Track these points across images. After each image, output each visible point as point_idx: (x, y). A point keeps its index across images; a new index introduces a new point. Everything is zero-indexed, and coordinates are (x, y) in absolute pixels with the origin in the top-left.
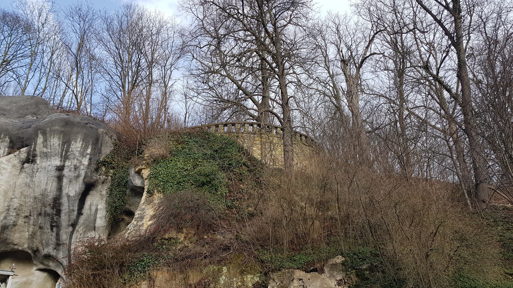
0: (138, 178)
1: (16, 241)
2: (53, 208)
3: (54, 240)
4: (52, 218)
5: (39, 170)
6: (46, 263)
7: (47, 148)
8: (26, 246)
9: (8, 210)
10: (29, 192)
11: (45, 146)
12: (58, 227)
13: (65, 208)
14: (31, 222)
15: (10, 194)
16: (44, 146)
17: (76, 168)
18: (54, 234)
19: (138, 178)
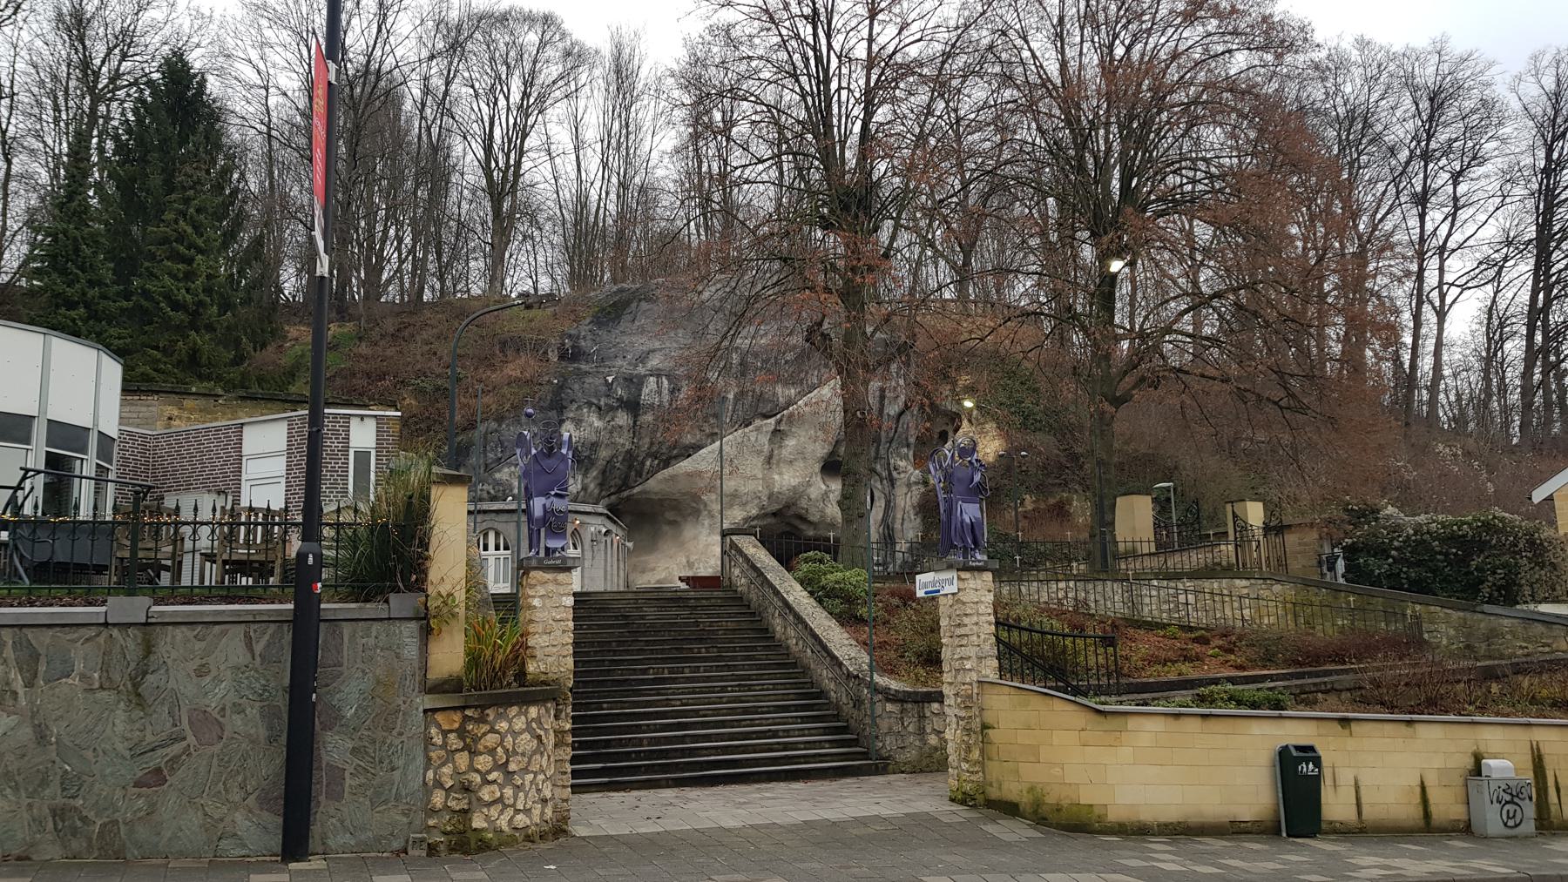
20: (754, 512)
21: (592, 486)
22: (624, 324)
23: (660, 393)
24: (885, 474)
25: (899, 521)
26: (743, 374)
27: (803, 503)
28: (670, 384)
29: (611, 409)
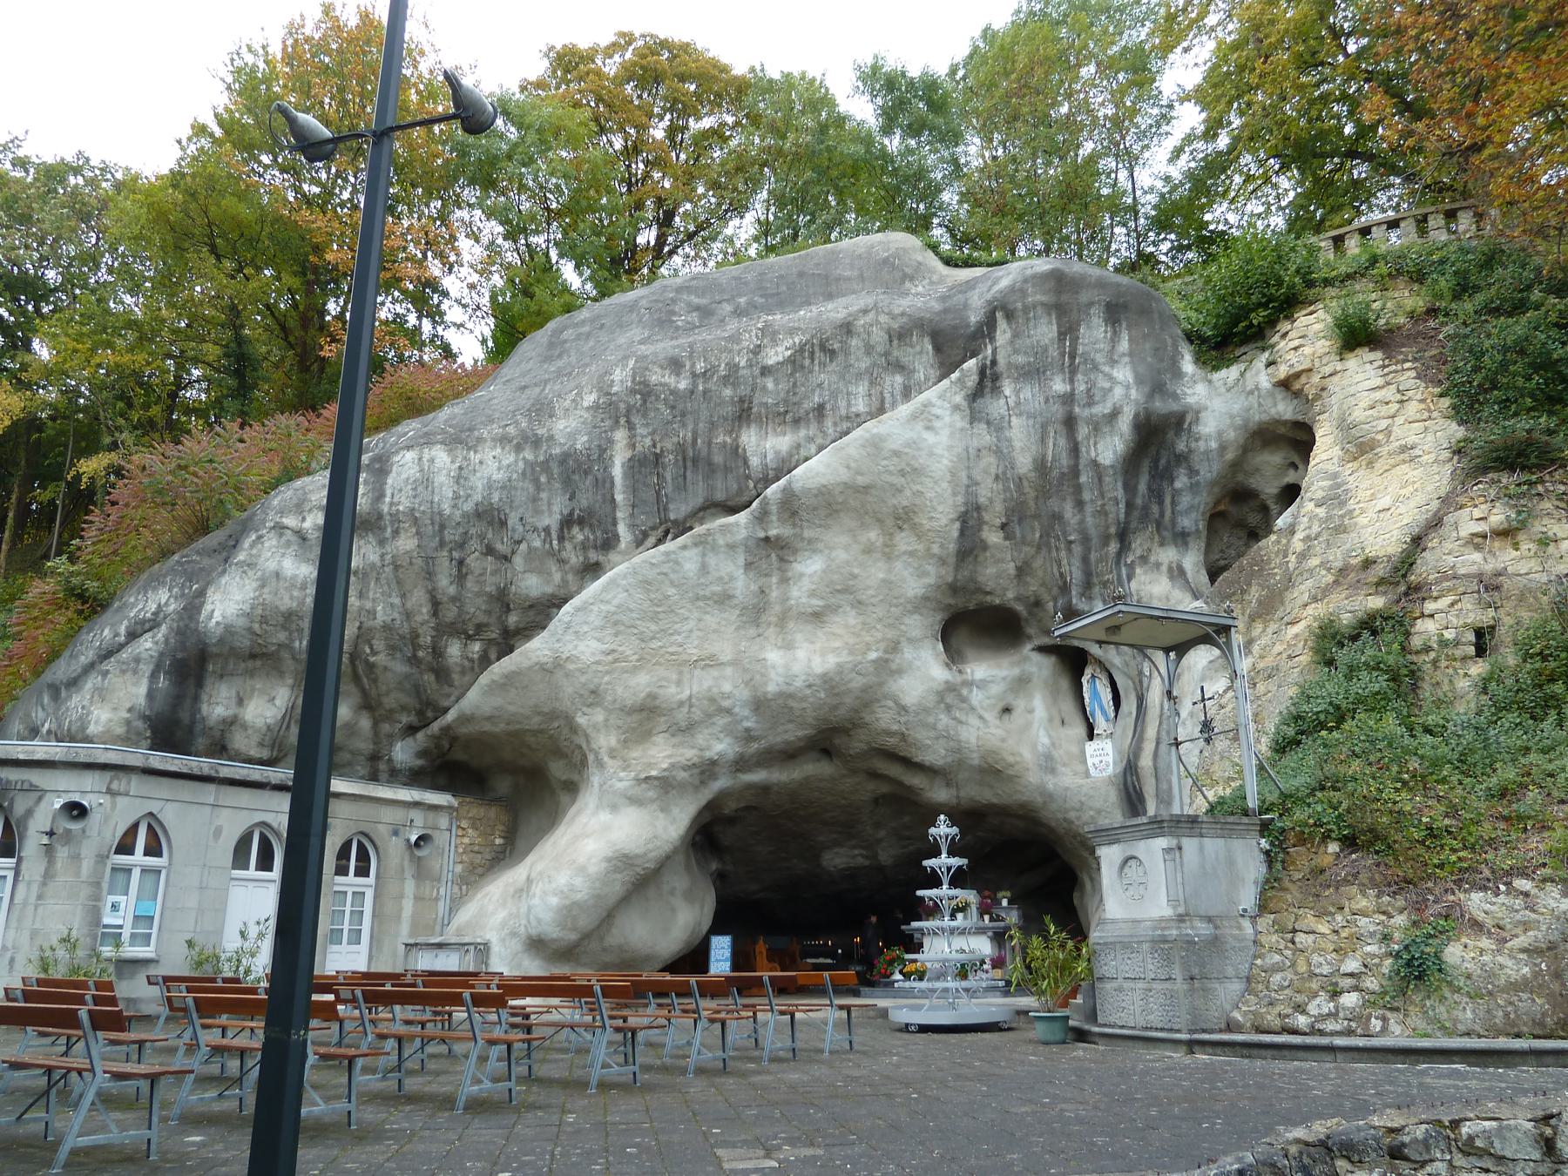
0: (1283, 399)
1: (990, 586)
18: (1077, 562)
19: (1283, 399)
27: (885, 718)
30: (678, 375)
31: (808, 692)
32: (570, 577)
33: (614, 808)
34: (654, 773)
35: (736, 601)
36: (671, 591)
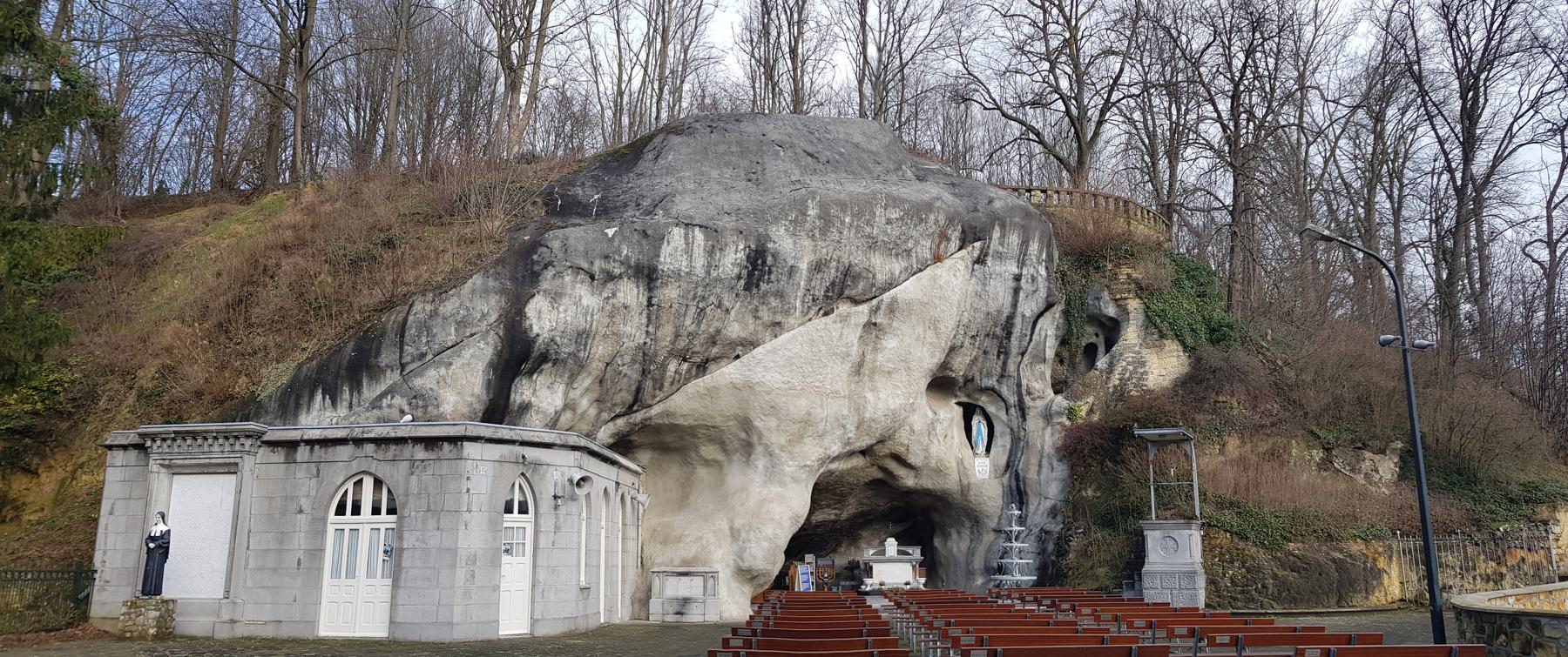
2: (1003, 330)
3: (999, 369)
4: (1001, 343)
5: (994, 276)
6: (978, 396)
7: (1003, 247)
8: (961, 373)
9: (958, 326)
10: (980, 304)
11: (1002, 244)
12: (1007, 354)
13: (1017, 331)
14: (977, 343)
15: (962, 305)
16: (1000, 244)
17: (1033, 279)
18: (1000, 363)
20: (836, 449)
21: (584, 403)
22: (645, 164)
23: (689, 252)
24: (1013, 399)
25: (1033, 469)
26: (824, 232)
27: (903, 436)
28: (707, 239)
29: (610, 277)
30: (845, 212)
31: (883, 419)
32: (760, 328)
33: (782, 484)
34: (809, 463)
35: (850, 358)
36: (823, 348)
